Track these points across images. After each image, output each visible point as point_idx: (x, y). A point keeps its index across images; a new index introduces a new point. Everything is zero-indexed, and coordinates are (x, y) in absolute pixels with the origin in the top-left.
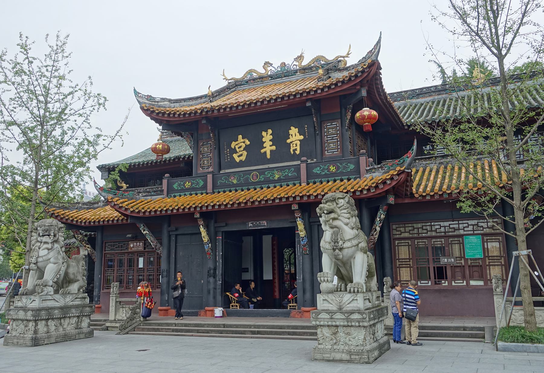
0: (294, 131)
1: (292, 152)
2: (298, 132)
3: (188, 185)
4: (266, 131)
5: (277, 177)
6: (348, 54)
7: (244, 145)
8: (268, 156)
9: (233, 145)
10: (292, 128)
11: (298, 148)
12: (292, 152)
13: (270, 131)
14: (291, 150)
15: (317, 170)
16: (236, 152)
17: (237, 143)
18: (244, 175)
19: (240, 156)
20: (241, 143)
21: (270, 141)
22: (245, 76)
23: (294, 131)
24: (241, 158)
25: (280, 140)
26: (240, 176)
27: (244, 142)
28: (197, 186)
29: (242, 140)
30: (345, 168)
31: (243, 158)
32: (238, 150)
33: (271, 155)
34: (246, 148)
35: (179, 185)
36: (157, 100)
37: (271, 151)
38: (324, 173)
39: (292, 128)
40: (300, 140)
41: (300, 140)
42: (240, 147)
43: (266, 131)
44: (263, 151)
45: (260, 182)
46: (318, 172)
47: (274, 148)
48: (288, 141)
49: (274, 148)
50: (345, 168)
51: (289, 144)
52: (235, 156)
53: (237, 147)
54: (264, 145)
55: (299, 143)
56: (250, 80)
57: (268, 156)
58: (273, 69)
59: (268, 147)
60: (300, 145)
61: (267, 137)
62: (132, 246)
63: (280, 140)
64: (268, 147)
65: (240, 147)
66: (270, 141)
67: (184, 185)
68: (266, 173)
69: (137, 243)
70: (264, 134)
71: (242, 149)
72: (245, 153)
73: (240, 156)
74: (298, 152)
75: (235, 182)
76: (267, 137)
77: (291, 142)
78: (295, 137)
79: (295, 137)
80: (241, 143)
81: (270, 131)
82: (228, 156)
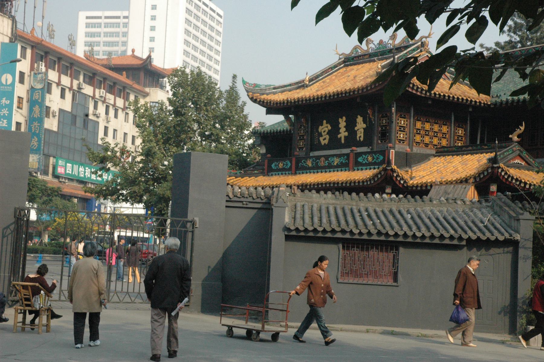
0: (360, 119)
1: (358, 139)
3: (281, 165)
4: (342, 118)
5: (335, 164)
6: (430, 35)
7: (326, 129)
8: (343, 142)
9: (320, 130)
10: (359, 117)
11: (362, 135)
13: (344, 118)
14: (358, 137)
15: (360, 160)
16: (322, 136)
17: (323, 127)
19: (324, 140)
20: (325, 128)
21: (345, 127)
22: (352, 52)
23: (360, 119)
24: (325, 141)
25: (351, 126)
26: (313, 160)
30: (378, 158)
31: (326, 142)
32: (323, 134)
33: (345, 140)
34: (329, 133)
35: (276, 165)
36: (263, 87)
37: (345, 137)
38: (364, 162)
39: (359, 117)
40: (364, 129)
41: (364, 129)
42: (324, 132)
43: (342, 118)
45: (326, 166)
46: (361, 161)
48: (356, 129)
49: (346, 134)
50: (378, 158)
51: (356, 132)
52: (321, 139)
54: (341, 131)
55: (362, 131)
56: (355, 57)
57: (343, 142)
58: (374, 46)
59: (343, 134)
61: (342, 123)
63: (351, 126)
64: (343, 134)
65: (324, 132)
68: (329, 159)
70: (340, 120)
71: (326, 133)
73: (324, 140)
74: (362, 139)
75: (310, 165)
76: (342, 123)
78: (360, 125)
79: (360, 125)
80: (325, 128)
81: (344, 118)
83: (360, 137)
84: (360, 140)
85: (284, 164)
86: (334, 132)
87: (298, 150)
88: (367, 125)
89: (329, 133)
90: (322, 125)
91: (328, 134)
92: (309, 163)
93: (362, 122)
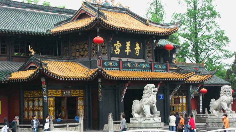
0: (137, 45)
1: (136, 55)
2: (139, 46)
4: (128, 42)
8: (128, 54)
11: (138, 53)
12: (136, 55)
13: (129, 42)
14: (136, 53)
16: (116, 49)
17: (116, 44)
18: (133, 63)
19: (117, 52)
20: (118, 45)
21: (129, 47)
23: (137, 45)
25: (132, 47)
27: (119, 45)
28: (115, 66)
29: (119, 44)
31: (118, 53)
32: (117, 48)
34: (120, 48)
37: (129, 52)
38: (157, 68)
39: (137, 43)
43: (128, 42)
44: (126, 51)
45: (138, 68)
47: (130, 50)
48: (135, 49)
52: (115, 51)
53: (116, 46)
54: (127, 48)
57: (128, 54)
59: (128, 50)
60: (139, 52)
61: (128, 45)
62: (64, 93)
64: (128, 50)
66: (129, 47)
67: (109, 64)
68: (140, 64)
69: (67, 91)
70: (127, 43)
71: (118, 48)
72: (119, 50)
74: (138, 55)
75: (130, 66)
76: (128, 45)
77: (136, 50)
78: (137, 48)
80: (118, 45)
81: (129, 42)
82: (112, 50)
83: (137, 53)
84: (137, 55)
85: (113, 64)
86: (123, 48)
87: (102, 55)
88: (141, 48)
89: (120, 48)
90: (116, 43)
91: (119, 48)
92: (129, 65)
93: (138, 46)
